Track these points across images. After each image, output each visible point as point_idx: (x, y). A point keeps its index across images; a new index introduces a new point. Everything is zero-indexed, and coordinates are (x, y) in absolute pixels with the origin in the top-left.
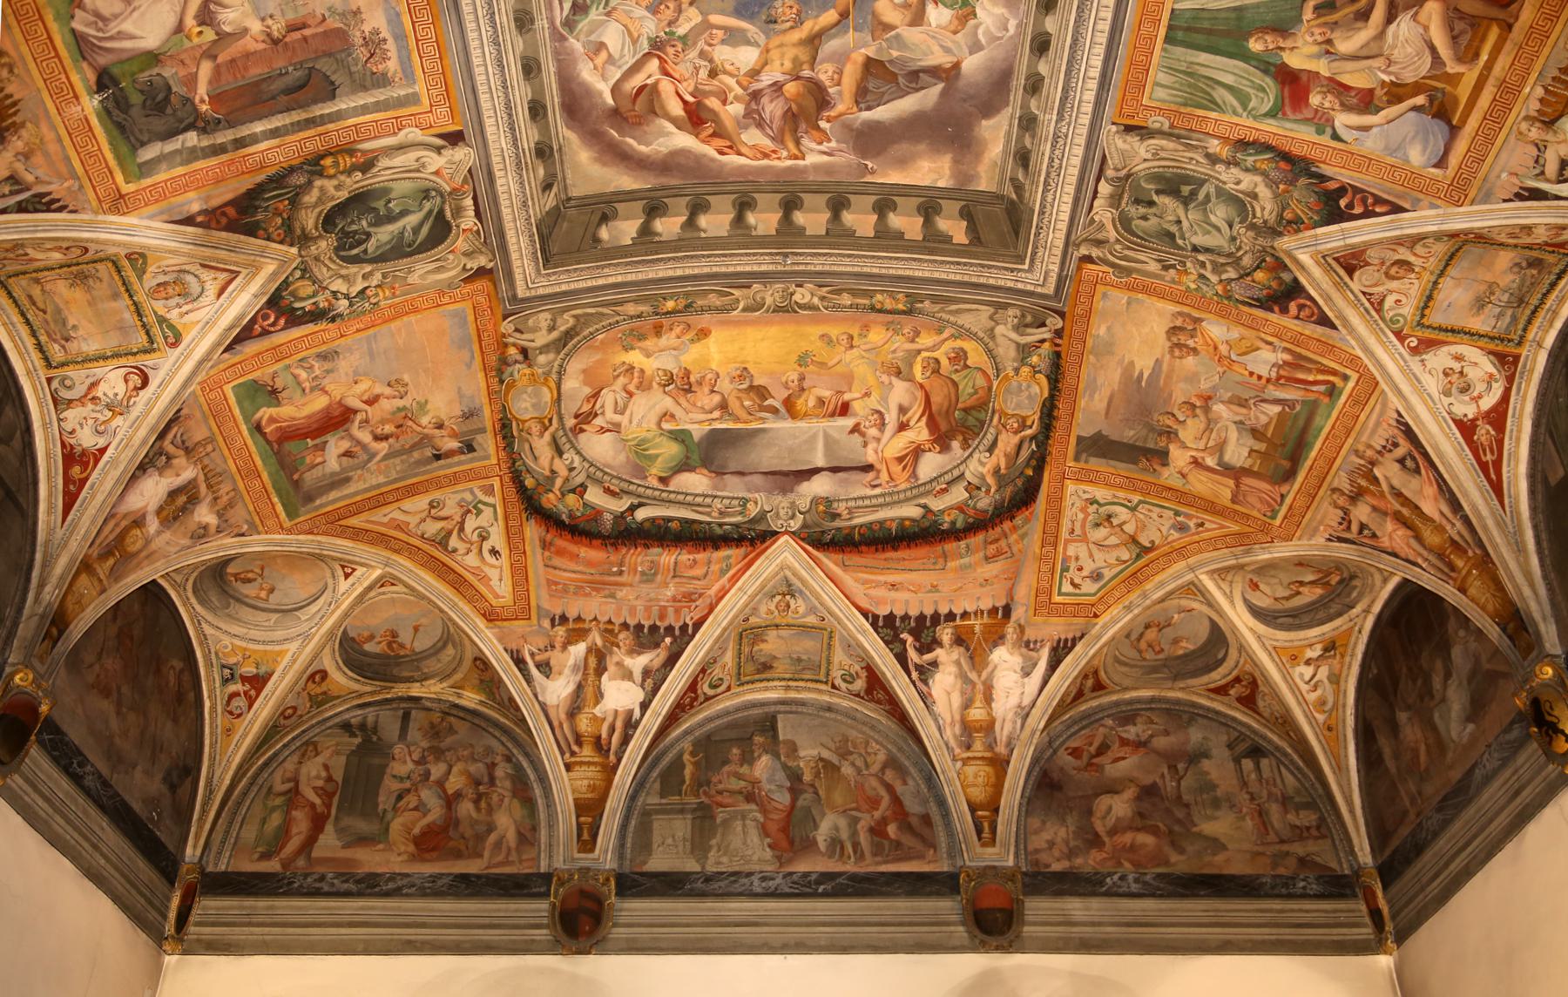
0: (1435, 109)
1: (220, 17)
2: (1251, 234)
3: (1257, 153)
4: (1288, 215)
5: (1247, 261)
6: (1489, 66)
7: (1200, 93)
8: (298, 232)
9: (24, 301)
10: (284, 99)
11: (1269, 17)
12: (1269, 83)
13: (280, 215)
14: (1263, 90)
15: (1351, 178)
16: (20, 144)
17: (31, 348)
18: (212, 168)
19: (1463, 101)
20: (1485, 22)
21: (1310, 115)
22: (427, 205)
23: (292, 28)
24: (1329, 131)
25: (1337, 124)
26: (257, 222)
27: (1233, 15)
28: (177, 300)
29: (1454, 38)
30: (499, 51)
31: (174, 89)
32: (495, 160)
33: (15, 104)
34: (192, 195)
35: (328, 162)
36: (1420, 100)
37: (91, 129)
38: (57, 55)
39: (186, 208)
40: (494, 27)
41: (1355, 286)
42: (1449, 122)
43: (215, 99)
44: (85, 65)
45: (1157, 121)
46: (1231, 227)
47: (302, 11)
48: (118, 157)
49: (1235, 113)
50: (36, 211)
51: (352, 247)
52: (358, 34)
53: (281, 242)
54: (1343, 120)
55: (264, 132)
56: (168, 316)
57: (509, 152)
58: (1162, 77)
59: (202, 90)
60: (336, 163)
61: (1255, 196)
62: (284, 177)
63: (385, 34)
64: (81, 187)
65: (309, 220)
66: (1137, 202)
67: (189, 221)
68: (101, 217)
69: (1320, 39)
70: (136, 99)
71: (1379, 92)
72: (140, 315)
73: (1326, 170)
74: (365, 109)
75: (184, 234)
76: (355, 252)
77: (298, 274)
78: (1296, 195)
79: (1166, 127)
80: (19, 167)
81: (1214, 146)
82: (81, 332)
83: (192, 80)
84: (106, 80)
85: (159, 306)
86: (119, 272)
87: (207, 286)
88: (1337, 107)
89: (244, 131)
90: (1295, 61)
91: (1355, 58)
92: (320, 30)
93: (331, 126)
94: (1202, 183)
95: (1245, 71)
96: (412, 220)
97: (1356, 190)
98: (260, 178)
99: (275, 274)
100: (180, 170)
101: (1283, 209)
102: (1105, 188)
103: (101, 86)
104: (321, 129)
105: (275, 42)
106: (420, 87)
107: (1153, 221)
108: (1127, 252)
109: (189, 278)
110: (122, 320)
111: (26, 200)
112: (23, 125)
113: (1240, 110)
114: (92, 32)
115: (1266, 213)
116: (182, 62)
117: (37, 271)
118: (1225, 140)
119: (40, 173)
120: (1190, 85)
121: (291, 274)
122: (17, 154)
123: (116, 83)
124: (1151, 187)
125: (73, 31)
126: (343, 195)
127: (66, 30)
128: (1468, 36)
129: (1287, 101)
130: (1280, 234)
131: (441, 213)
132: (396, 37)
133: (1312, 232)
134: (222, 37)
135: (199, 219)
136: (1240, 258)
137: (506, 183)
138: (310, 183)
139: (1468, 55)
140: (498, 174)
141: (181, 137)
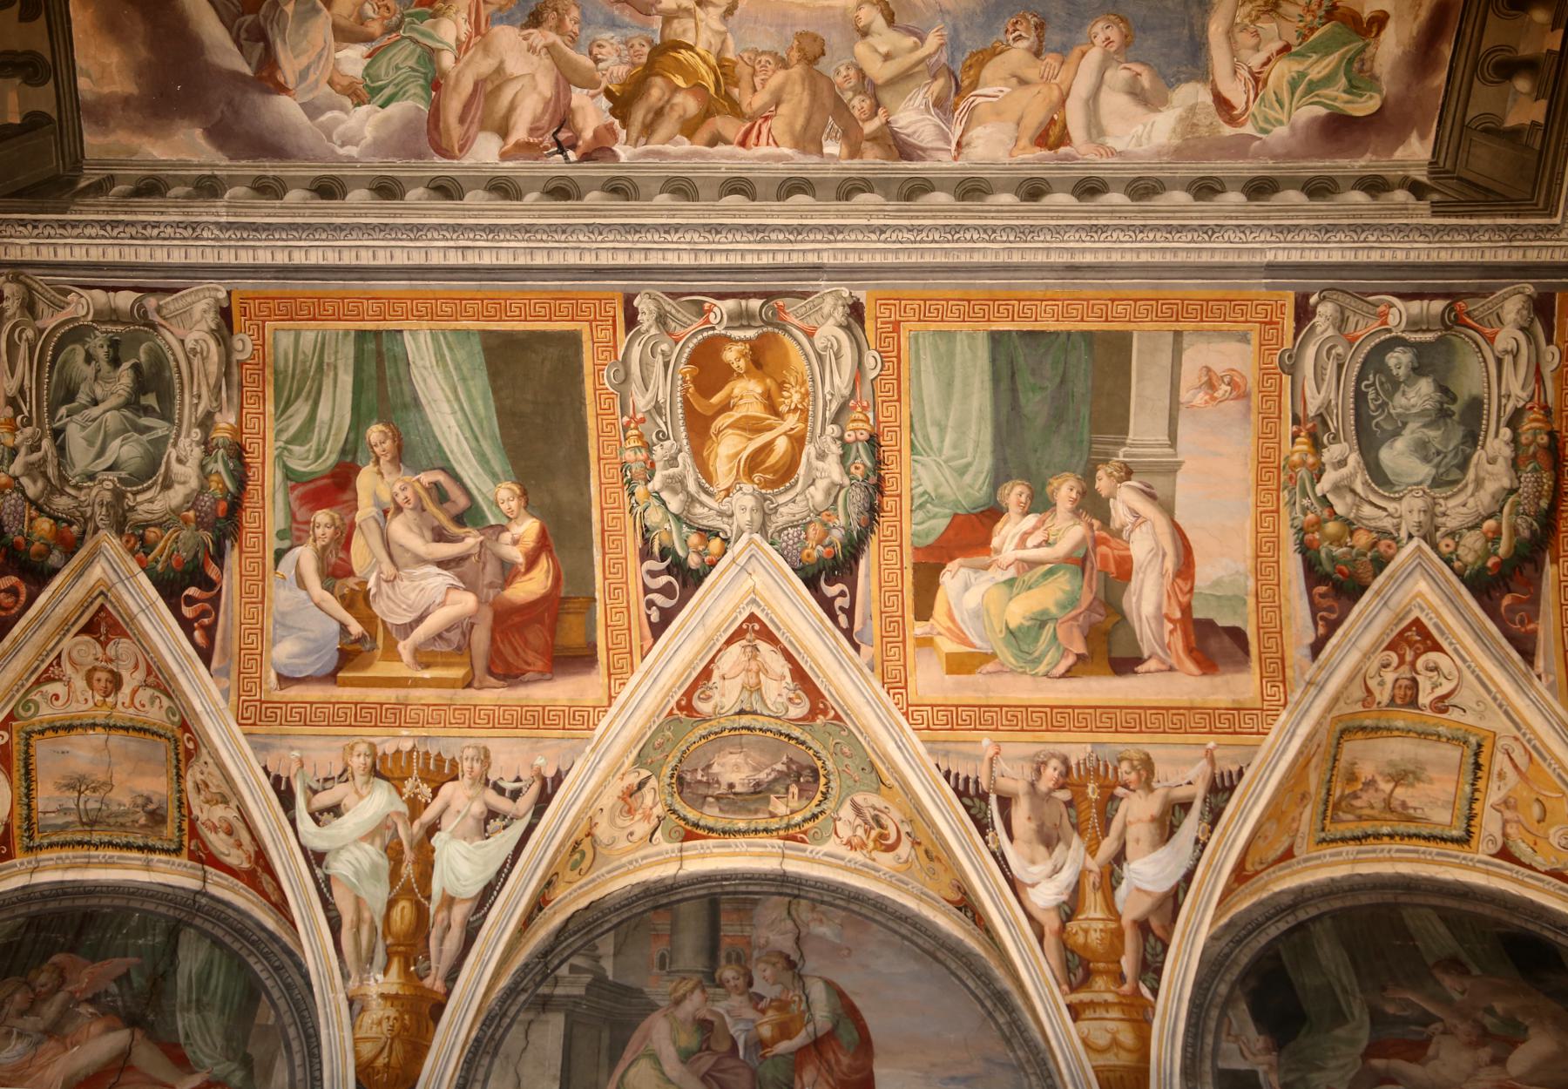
0: (349, 648)
2: (108, 496)
3: (231, 473)
4: (151, 533)
5: (61, 503)
6: (418, 683)
7: (294, 386)
11: (415, 438)
12: (330, 459)
14: (319, 455)
15: (230, 589)
19: (369, 673)
20: (467, 660)
21: (299, 518)
24: (286, 544)
25: (298, 550)
27: (408, 399)
29: (440, 636)
36: (356, 628)
41: (67, 642)
42: (338, 669)
45: (243, 345)
46: (110, 469)
49: (279, 432)
54: (306, 556)
58: (308, 338)
61: (167, 485)
66: (114, 344)
69: (400, 499)
71: (351, 582)
73: (232, 558)
78: (185, 534)
79: (238, 357)
81: (226, 420)
88: (320, 543)
90: (366, 481)
91: (387, 543)
94: (166, 416)
95: (339, 428)
97: (215, 602)
101: (159, 525)
102: (125, 300)
107: (89, 371)
108: (24, 347)
113: (285, 437)
115: (146, 506)
118: (239, 429)
120: (305, 372)
124: (143, 358)
128: (445, 649)
129: (312, 486)
130: (120, 533)
133: (136, 569)
136: (62, 493)
139: (424, 657)
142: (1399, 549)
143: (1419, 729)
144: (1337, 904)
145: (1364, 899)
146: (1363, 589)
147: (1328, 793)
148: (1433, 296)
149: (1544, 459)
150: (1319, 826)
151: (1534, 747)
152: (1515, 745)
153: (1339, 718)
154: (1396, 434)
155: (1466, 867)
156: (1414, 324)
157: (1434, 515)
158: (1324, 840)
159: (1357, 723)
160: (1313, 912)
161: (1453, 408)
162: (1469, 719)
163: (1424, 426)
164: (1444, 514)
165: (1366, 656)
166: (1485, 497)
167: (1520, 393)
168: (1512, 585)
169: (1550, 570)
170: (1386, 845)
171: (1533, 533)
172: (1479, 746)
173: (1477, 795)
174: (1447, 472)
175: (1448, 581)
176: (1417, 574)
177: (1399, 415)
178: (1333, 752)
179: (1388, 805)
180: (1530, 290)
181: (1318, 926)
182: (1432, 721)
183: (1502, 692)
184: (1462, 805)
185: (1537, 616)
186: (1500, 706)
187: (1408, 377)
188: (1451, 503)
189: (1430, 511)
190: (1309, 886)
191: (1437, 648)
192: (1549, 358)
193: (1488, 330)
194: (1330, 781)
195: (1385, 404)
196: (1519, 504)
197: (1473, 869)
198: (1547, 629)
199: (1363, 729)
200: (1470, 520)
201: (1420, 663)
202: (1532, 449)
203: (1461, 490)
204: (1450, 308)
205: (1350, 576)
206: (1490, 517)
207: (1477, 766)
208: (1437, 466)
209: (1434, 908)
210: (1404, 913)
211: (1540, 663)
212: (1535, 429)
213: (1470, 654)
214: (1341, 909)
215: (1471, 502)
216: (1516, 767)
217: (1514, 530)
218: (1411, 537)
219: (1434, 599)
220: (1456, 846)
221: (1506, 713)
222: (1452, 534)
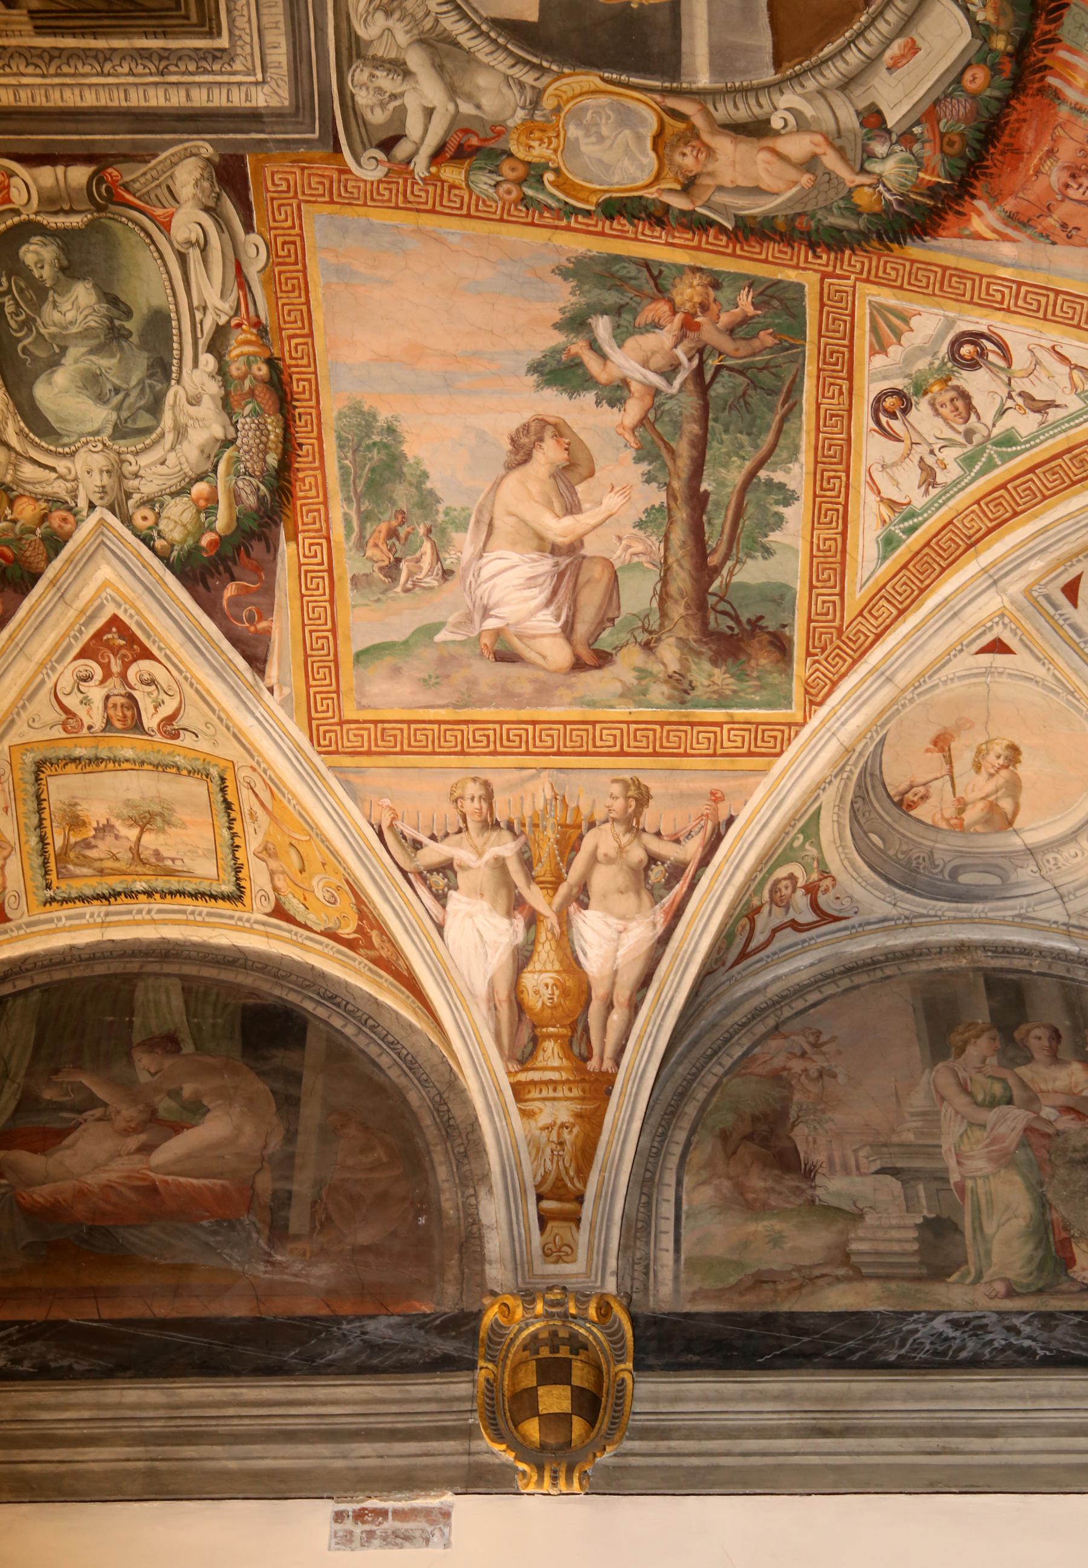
142: (77, 523)
143: (154, 758)
144: (60, 975)
145: (100, 969)
146: (35, 577)
147: (42, 839)
148: (70, 160)
149: (266, 398)
150: (40, 882)
151: (270, 778)
152: (255, 776)
153: (27, 747)
154: (54, 363)
155: (243, 929)
156: (52, 202)
157: (122, 477)
158: (52, 900)
159: (61, 753)
160: (22, 984)
161: (127, 325)
162: (203, 745)
163: (92, 352)
164: (136, 475)
165: (48, 664)
166: (191, 452)
167: (219, 304)
168: (236, 571)
169: (286, 550)
170: (143, 904)
171: (261, 500)
172: (223, 779)
173: (237, 841)
174: (133, 416)
175: (145, 565)
176: (98, 556)
177: (53, 336)
178: (31, 789)
179: (136, 851)
180: (207, 150)
181: (20, 1001)
182: (166, 750)
183: (223, 709)
184: (225, 851)
185: (271, 611)
186: (228, 728)
187: (57, 281)
188: (144, 460)
189: (116, 471)
190: (36, 955)
191: (147, 655)
192: (252, 251)
193: (159, 212)
194: (40, 825)
195: (28, 324)
196: (238, 460)
197: (251, 930)
198: (284, 628)
199: (76, 760)
200: (174, 483)
201: (132, 674)
202: (247, 384)
203: (155, 443)
204: (97, 178)
205: (15, 560)
206: (200, 478)
207: (228, 806)
208: (118, 408)
209: (183, 978)
210: (141, 985)
211: (273, 671)
212: (248, 355)
213: (182, 662)
214: (62, 980)
215: (172, 459)
216: (262, 804)
217: (235, 497)
218: (92, 506)
219: (128, 587)
220: (227, 904)
221: (235, 736)
222: (148, 502)
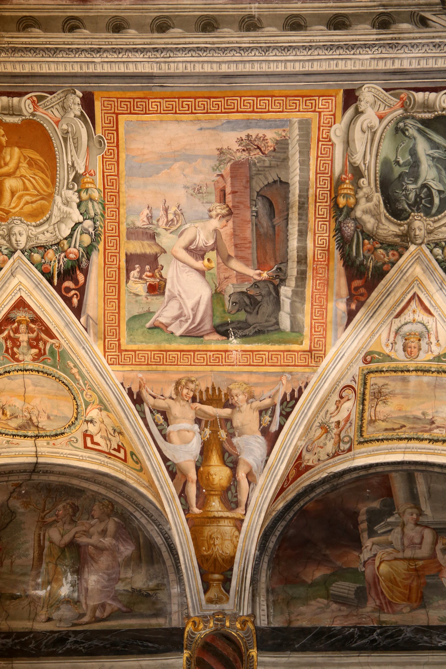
1: (201, 244)
8: (397, 240)
9: (389, 434)
10: (277, 220)
13: (376, 249)
16: (241, 397)
17: (431, 446)
18: (314, 286)
22: (412, 132)
23: (223, 198)
26: (374, 267)
28: (423, 343)
30: (275, 48)
31: (244, 290)
32: (381, 66)
33: (214, 389)
34: (331, 306)
35: (342, 201)
37: (252, 351)
38: (194, 351)
39: (339, 313)
40: (252, 49)
43: (261, 266)
44: (206, 338)
47: (212, 188)
48: (280, 342)
50: (293, 407)
51: (431, 202)
52: (239, 154)
53: (401, 255)
55: (299, 241)
56: (436, 354)
57: (376, 53)
59: (252, 273)
60: (346, 196)
62: (342, 237)
63: (243, 135)
64: (291, 373)
65: (390, 229)
67: (351, 315)
68: (320, 370)
70: (242, 316)
72: (428, 371)
74: (304, 164)
75: (359, 321)
76: (437, 201)
77: (438, 251)
80: (256, 404)
82: (430, 412)
83: (241, 277)
84: (222, 329)
85: (423, 356)
86: (381, 371)
87: (420, 319)
89: (293, 254)
92: (229, 180)
93: (311, 192)
96: (422, 147)
98: (337, 254)
99: (427, 269)
100: (307, 306)
103: (225, 334)
104: (311, 200)
105: (230, 213)
106: (295, 117)
109: (406, 329)
110: (428, 384)
111: (282, 410)
112: (229, 390)
114: (186, 326)
116: (226, 278)
117: (362, 418)
119: (267, 394)
121: (435, 256)
122: (247, 401)
123: (227, 324)
125: (181, 336)
126: (377, 197)
127: (180, 340)
131: (424, 122)
132: (248, 127)
134: (215, 247)
135: (353, 307)
137: (409, 59)
138: (355, 219)
140: (397, 65)
141: (282, 297)
